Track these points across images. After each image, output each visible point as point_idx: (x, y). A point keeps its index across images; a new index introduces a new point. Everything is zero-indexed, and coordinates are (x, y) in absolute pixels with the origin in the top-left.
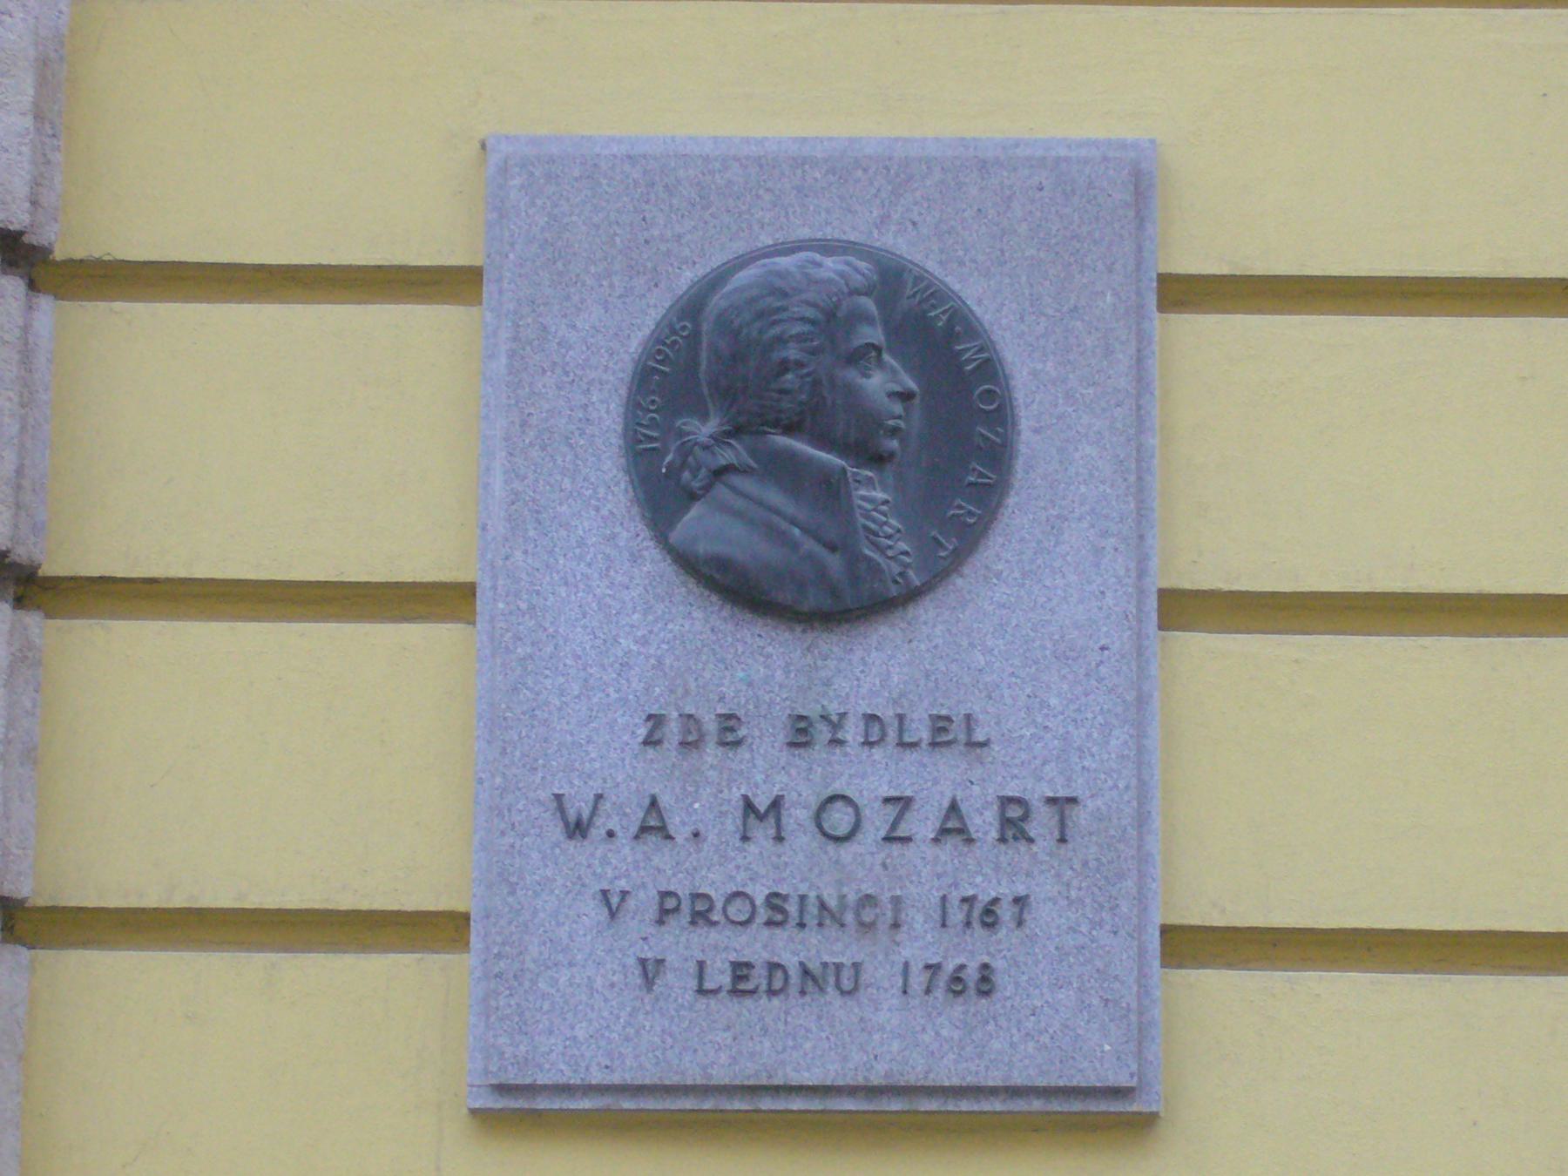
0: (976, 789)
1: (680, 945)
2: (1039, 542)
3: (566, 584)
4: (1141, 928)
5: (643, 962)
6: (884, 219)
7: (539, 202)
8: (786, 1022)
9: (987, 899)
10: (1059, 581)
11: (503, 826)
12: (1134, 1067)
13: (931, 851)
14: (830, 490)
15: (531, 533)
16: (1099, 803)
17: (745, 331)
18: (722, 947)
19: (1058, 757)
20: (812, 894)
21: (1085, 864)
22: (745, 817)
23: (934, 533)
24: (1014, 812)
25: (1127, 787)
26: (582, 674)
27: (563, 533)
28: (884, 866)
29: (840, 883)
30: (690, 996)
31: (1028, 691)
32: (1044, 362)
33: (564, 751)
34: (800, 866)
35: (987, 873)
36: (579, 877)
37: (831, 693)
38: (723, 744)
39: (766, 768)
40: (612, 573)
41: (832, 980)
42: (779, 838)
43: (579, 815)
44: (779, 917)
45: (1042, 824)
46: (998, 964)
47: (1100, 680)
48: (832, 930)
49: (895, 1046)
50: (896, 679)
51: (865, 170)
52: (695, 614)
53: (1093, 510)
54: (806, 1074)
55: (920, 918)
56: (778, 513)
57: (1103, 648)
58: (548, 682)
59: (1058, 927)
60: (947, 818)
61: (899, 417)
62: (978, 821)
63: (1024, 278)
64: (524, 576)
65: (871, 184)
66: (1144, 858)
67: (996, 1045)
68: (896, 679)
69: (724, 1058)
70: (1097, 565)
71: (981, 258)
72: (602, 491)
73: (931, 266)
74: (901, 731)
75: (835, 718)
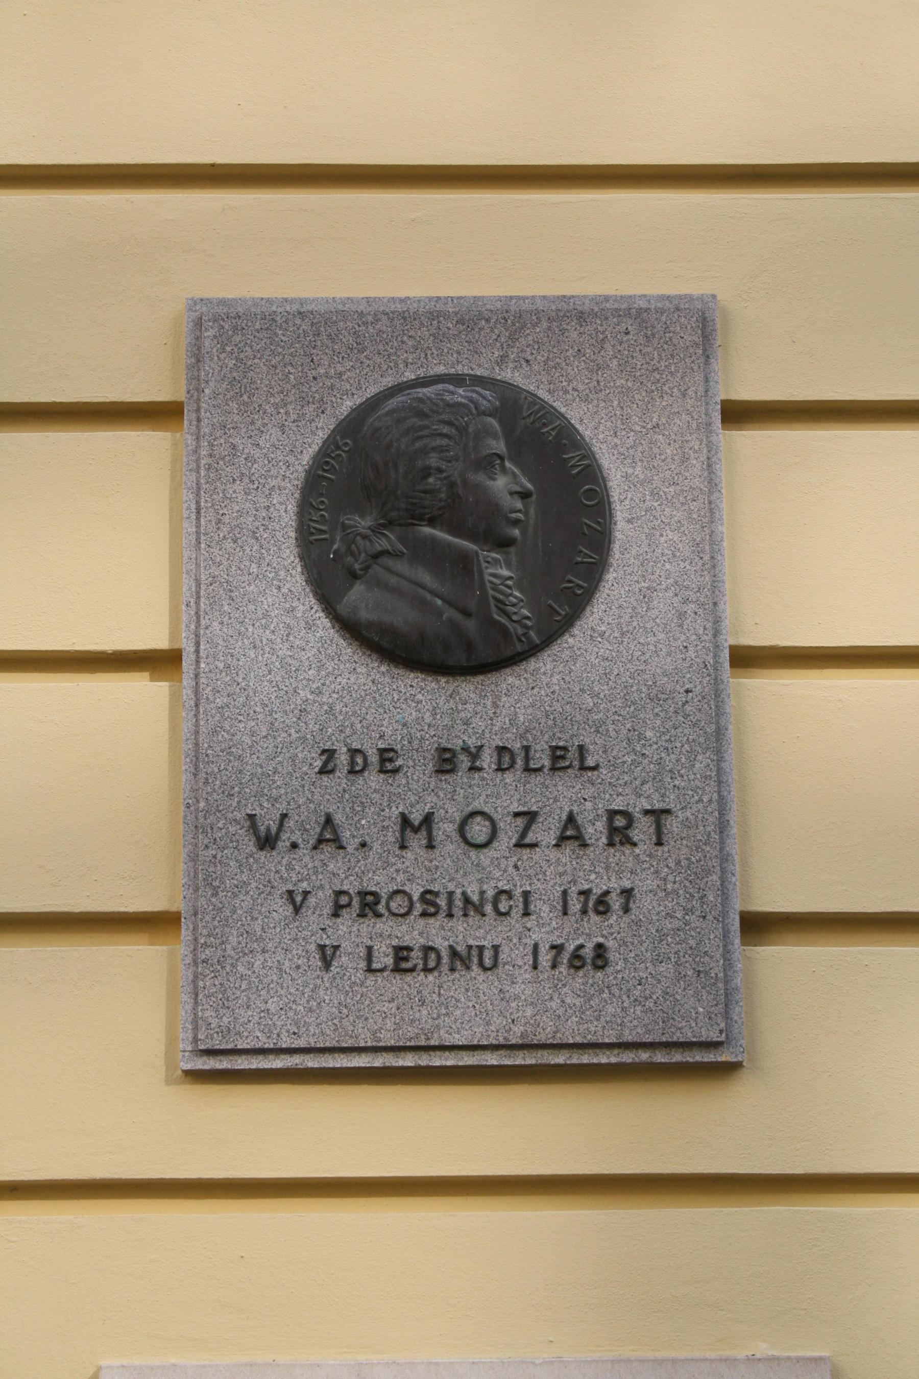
0: (589, 805)
1: (350, 932)
2: (634, 608)
3: (255, 647)
4: (724, 914)
5: (322, 948)
6: (503, 358)
7: (228, 349)
8: (439, 994)
9: (599, 892)
10: (651, 639)
11: (206, 841)
12: (723, 1025)
13: (553, 854)
14: (465, 565)
15: (226, 608)
16: (688, 814)
17: (395, 444)
18: (386, 933)
19: (654, 779)
20: (459, 891)
21: (678, 863)
22: (403, 831)
23: (550, 602)
24: (620, 822)
25: (710, 801)
26: (269, 718)
27: (251, 607)
28: (516, 867)
29: (480, 881)
30: (360, 975)
31: (628, 726)
32: (634, 468)
33: (255, 780)
34: (449, 868)
35: (600, 871)
36: (269, 881)
37: (470, 731)
38: (381, 771)
39: (417, 791)
40: (291, 638)
41: (475, 960)
42: (430, 846)
43: (268, 829)
44: (432, 910)
45: (642, 831)
46: (610, 944)
47: (686, 716)
48: (474, 919)
49: (529, 1012)
50: (522, 719)
51: (488, 321)
52: (359, 670)
53: (676, 583)
54: (457, 1036)
55: (546, 908)
56: (424, 587)
57: (687, 691)
58: (242, 725)
59: (658, 913)
60: (565, 828)
61: (519, 511)
62: (591, 830)
63: (616, 403)
64: (221, 642)
65: (492, 331)
66: (725, 858)
67: (610, 1009)
68: (522, 719)
69: (389, 1025)
70: (681, 626)
71: (581, 387)
72: (282, 573)
73: (542, 394)
74: (527, 759)
75: (473, 750)
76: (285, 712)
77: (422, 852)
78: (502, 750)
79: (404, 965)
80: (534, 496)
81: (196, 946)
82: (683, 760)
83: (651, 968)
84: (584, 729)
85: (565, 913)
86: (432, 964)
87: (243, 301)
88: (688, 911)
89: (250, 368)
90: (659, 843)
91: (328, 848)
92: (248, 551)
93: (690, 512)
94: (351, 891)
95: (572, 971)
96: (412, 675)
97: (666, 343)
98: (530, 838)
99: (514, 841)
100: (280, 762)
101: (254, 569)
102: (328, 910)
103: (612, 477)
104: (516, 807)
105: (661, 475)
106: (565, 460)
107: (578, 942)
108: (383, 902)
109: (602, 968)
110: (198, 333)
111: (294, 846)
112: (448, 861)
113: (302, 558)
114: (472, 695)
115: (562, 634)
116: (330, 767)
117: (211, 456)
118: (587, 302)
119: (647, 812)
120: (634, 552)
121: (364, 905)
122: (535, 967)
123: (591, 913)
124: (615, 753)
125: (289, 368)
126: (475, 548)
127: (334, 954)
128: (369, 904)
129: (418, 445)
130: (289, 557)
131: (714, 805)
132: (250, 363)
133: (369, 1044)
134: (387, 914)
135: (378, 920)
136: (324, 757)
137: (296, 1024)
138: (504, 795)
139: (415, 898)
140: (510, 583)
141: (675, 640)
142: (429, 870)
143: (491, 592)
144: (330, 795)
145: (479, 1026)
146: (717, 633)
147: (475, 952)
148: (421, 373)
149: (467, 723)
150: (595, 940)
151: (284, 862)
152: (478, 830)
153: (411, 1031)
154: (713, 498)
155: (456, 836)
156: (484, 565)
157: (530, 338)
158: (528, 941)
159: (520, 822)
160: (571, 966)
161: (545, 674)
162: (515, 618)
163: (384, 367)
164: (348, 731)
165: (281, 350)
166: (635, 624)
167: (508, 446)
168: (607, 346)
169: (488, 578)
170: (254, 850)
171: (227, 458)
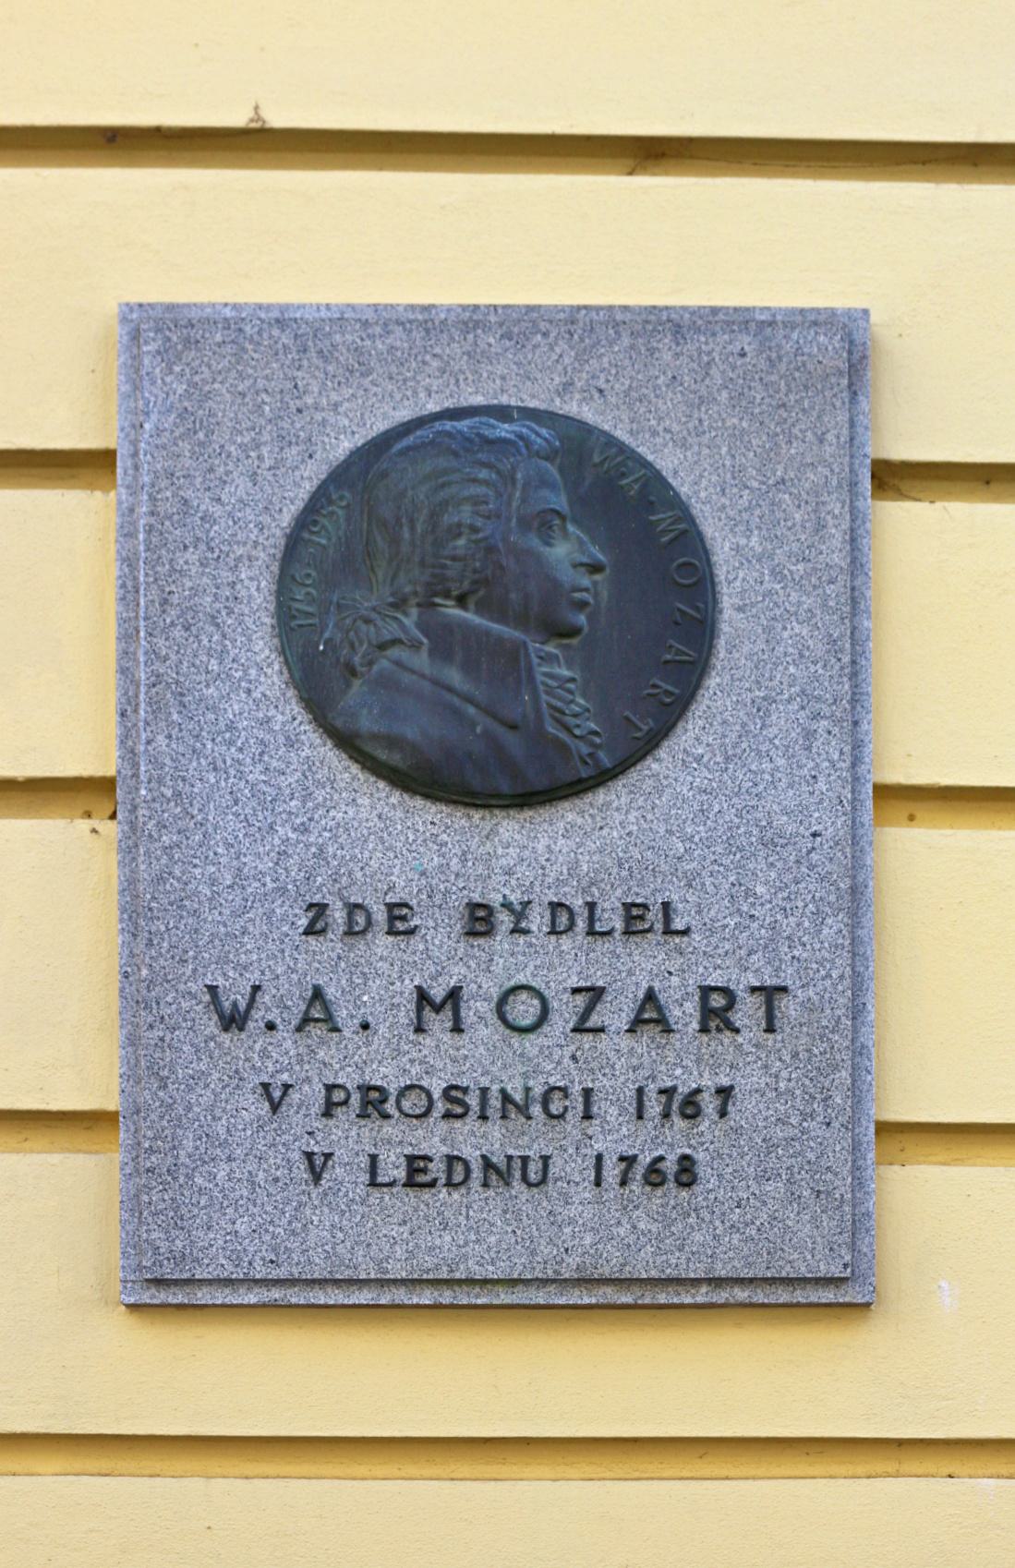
0: (675, 980)
1: (349, 1139)
2: (744, 725)
3: (215, 769)
4: (853, 1122)
5: (309, 1156)
6: (567, 386)
7: (177, 369)
8: (467, 1217)
9: (686, 1090)
10: (766, 766)
11: (150, 1019)
12: (848, 1258)
13: (625, 1042)
14: (511, 663)
15: (175, 716)
16: (811, 993)
18: (394, 1141)
19: (766, 947)
20: (495, 1087)
21: (795, 1055)
22: (419, 1010)
23: (627, 713)
24: (717, 1001)
25: (842, 977)
26: (235, 863)
27: (211, 716)
28: (574, 1058)
29: (525, 1075)
30: (362, 1190)
31: (732, 879)
32: (748, 537)
33: (217, 942)
34: (481, 1055)
35: (687, 1062)
36: (237, 1072)
37: (513, 882)
38: (392, 932)
39: (441, 954)
40: (266, 758)
41: (517, 1174)
42: (457, 1029)
43: (235, 1004)
44: (459, 1110)
45: (748, 1012)
46: (700, 1156)
47: (812, 867)
48: (516, 1119)
49: (588, 1240)
50: (585, 868)
51: (545, 335)
52: (359, 801)
53: (803, 691)
54: (491, 1268)
55: (614, 1111)
56: (450, 689)
57: (814, 835)
58: (197, 871)
59: (766, 1119)
60: (642, 1009)
61: (586, 590)
62: (677, 1012)
63: (724, 450)
64: (167, 761)
65: (552, 349)
66: (859, 1052)
67: (698, 1237)
68: (585, 868)
69: (399, 1251)
70: (809, 748)
71: (675, 428)
72: (253, 672)
73: (621, 434)
74: (591, 920)
75: (518, 908)
76: (258, 855)
77: (447, 1037)
78: (555, 907)
79: (422, 1178)
80: (608, 571)
81: (136, 1149)
82: (807, 924)
83: (754, 1188)
84: (671, 882)
85: (640, 1117)
86: (458, 1178)
87: (202, 306)
88: (805, 1116)
89: (207, 396)
90: (770, 1029)
91: (316, 1031)
92: (205, 642)
93: (826, 598)
94: (349, 1086)
95: (648, 1188)
96: (434, 809)
97: (798, 369)
98: (594, 1021)
99: (571, 1025)
100: (250, 920)
101: (214, 665)
102: (317, 1108)
103: (717, 550)
104: (574, 982)
105: (786, 548)
106: (651, 522)
107: (656, 1154)
108: (392, 1100)
109: (688, 1185)
110: (135, 351)
111: (271, 1026)
112: (482, 1049)
113: (282, 652)
114: (517, 837)
115: (643, 757)
116: (319, 926)
117: (152, 514)
118: (687, 316)
119: (754, 990)
120: (745, 650)
121: (366, 1103)
122: (598, 1184)
123: (676, 1119)
124: (712, 913)
125: (264, 396)
126: (523, 637)
127: (325, 1163)
128: (373, 1101)
129: (442, 494)
130: (262, 650)
131: (847, 982)
132: (207, 388)
133: (372, 1276)
134: (397, 1114)
135: (385, 1123)
136: (310, 914)
137: (274, 1250)
138: (560, 966)
139: (436, 1096)
140: (571, 686)
141: (800, 767)
142: (454, 1060)
143: (544, 697)
144: (323, 961)
145: (521, 1256)
146: (856, 762)
147: (517, 1164)
148: (449, 404)
149: (509, 872)
150: (679, 1151)
151: (257, 1047)
152: (524, 1010)
153: (430, 1262)
154: (857, 583)
155: (493, 1018)
156: (535, 660)
157: (605, 360)
158: (589, 1151)
159: (581, 1000)
160: (647, 1181)
161: (618, 809)
162: (577, 732)
163: (398, 396)
164: (344, 880)
165: (250, 371)
166: (744, 745)
167: (571, 504)
168: (714, 371)
169: (539, 678)
170: (216, 1032)
171: (176, 517)
